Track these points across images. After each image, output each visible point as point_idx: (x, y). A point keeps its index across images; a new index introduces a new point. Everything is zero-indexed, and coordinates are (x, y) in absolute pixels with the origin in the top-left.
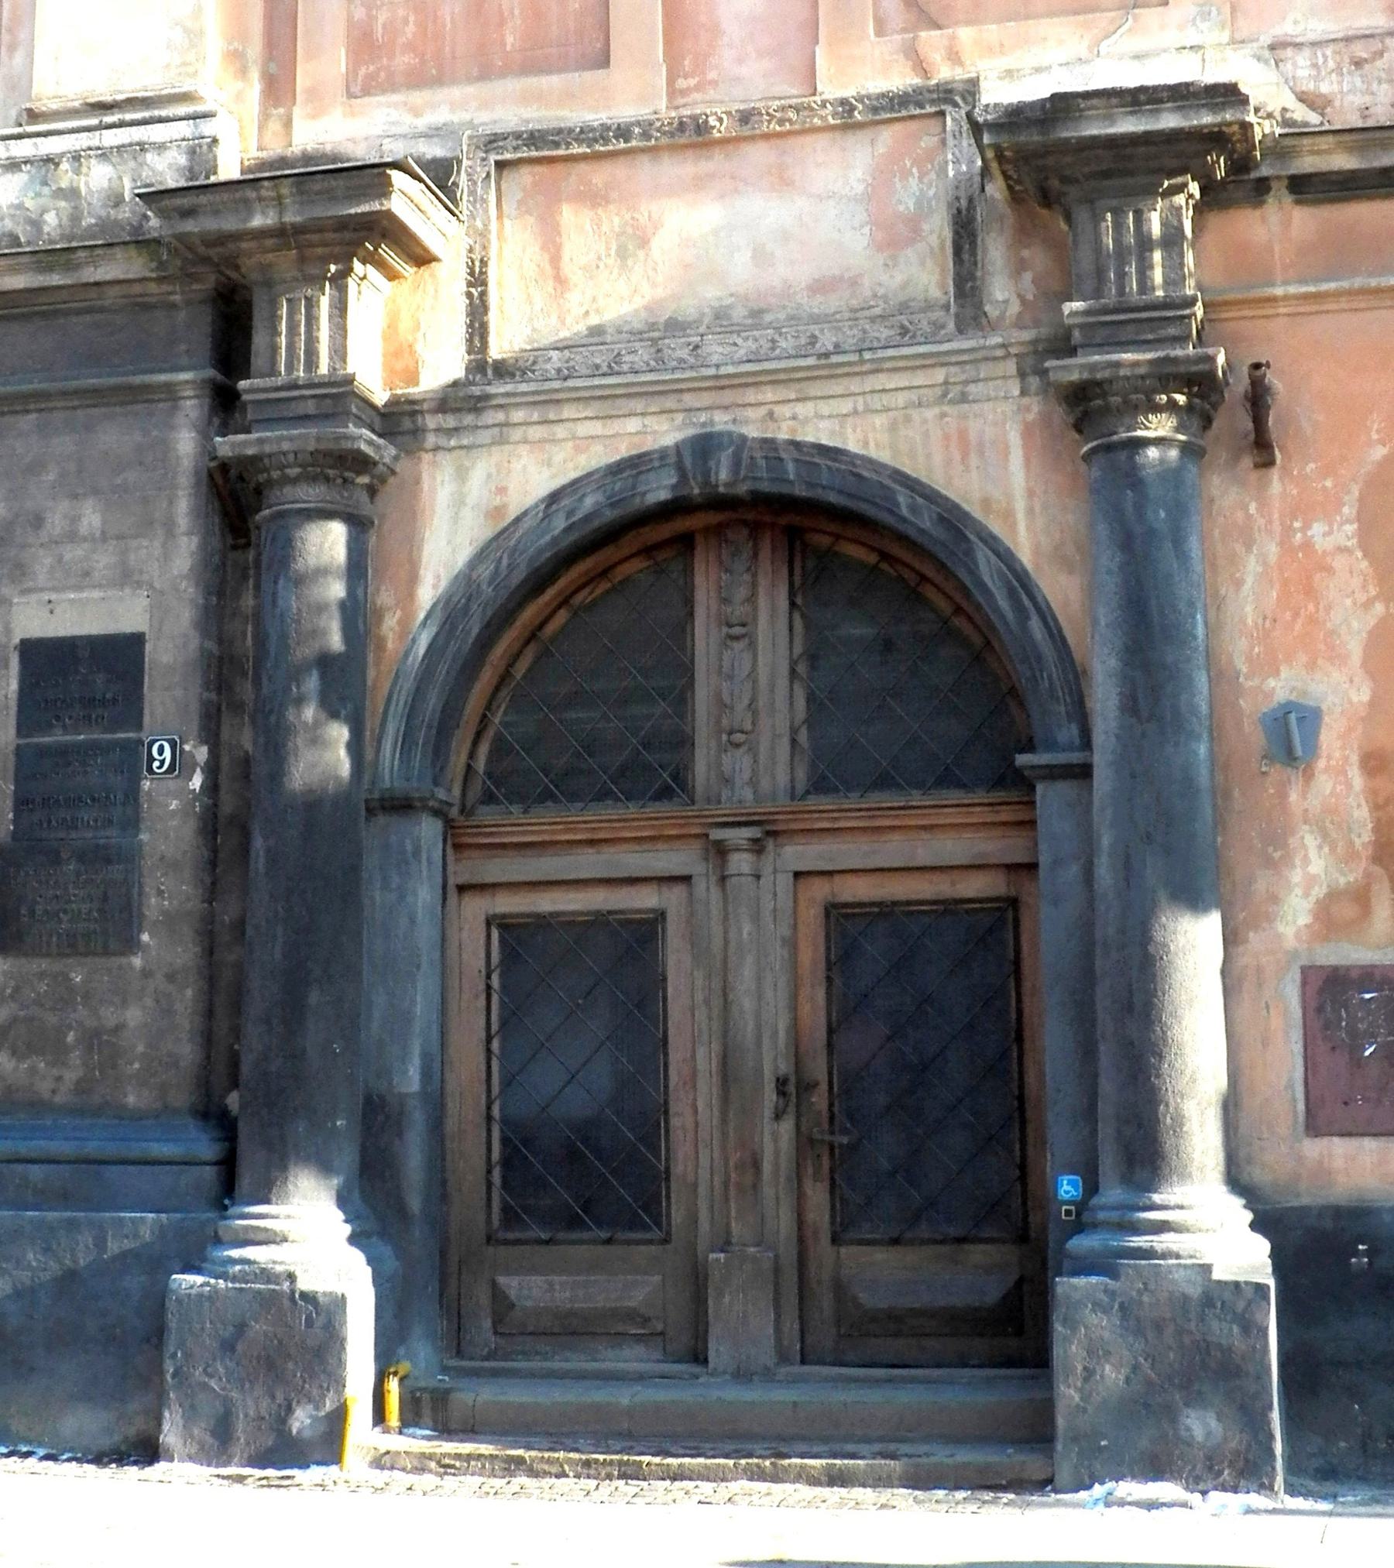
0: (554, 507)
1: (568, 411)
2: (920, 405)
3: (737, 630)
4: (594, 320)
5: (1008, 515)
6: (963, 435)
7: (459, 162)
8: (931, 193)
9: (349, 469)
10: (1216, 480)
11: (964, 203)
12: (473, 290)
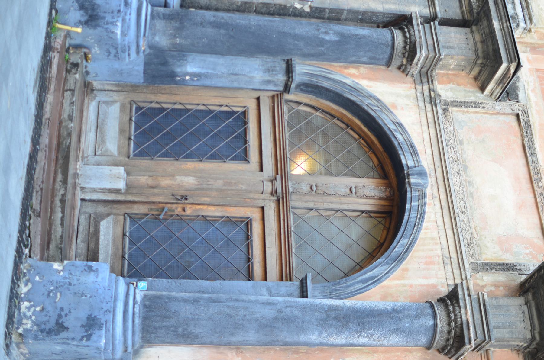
0: (397, 125)
1: (432, 131)
2: (442, 248)
3: (353, 190)
4: (465, 142)
5: (402, 277)
6: (432, 263)
7: (517, 102)
8: (521, 257)
9: (409, 54)
10: (419, 354)
11: (518, 267)
12: (473, 104)
